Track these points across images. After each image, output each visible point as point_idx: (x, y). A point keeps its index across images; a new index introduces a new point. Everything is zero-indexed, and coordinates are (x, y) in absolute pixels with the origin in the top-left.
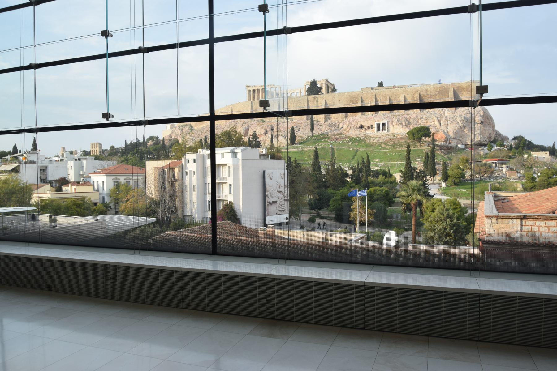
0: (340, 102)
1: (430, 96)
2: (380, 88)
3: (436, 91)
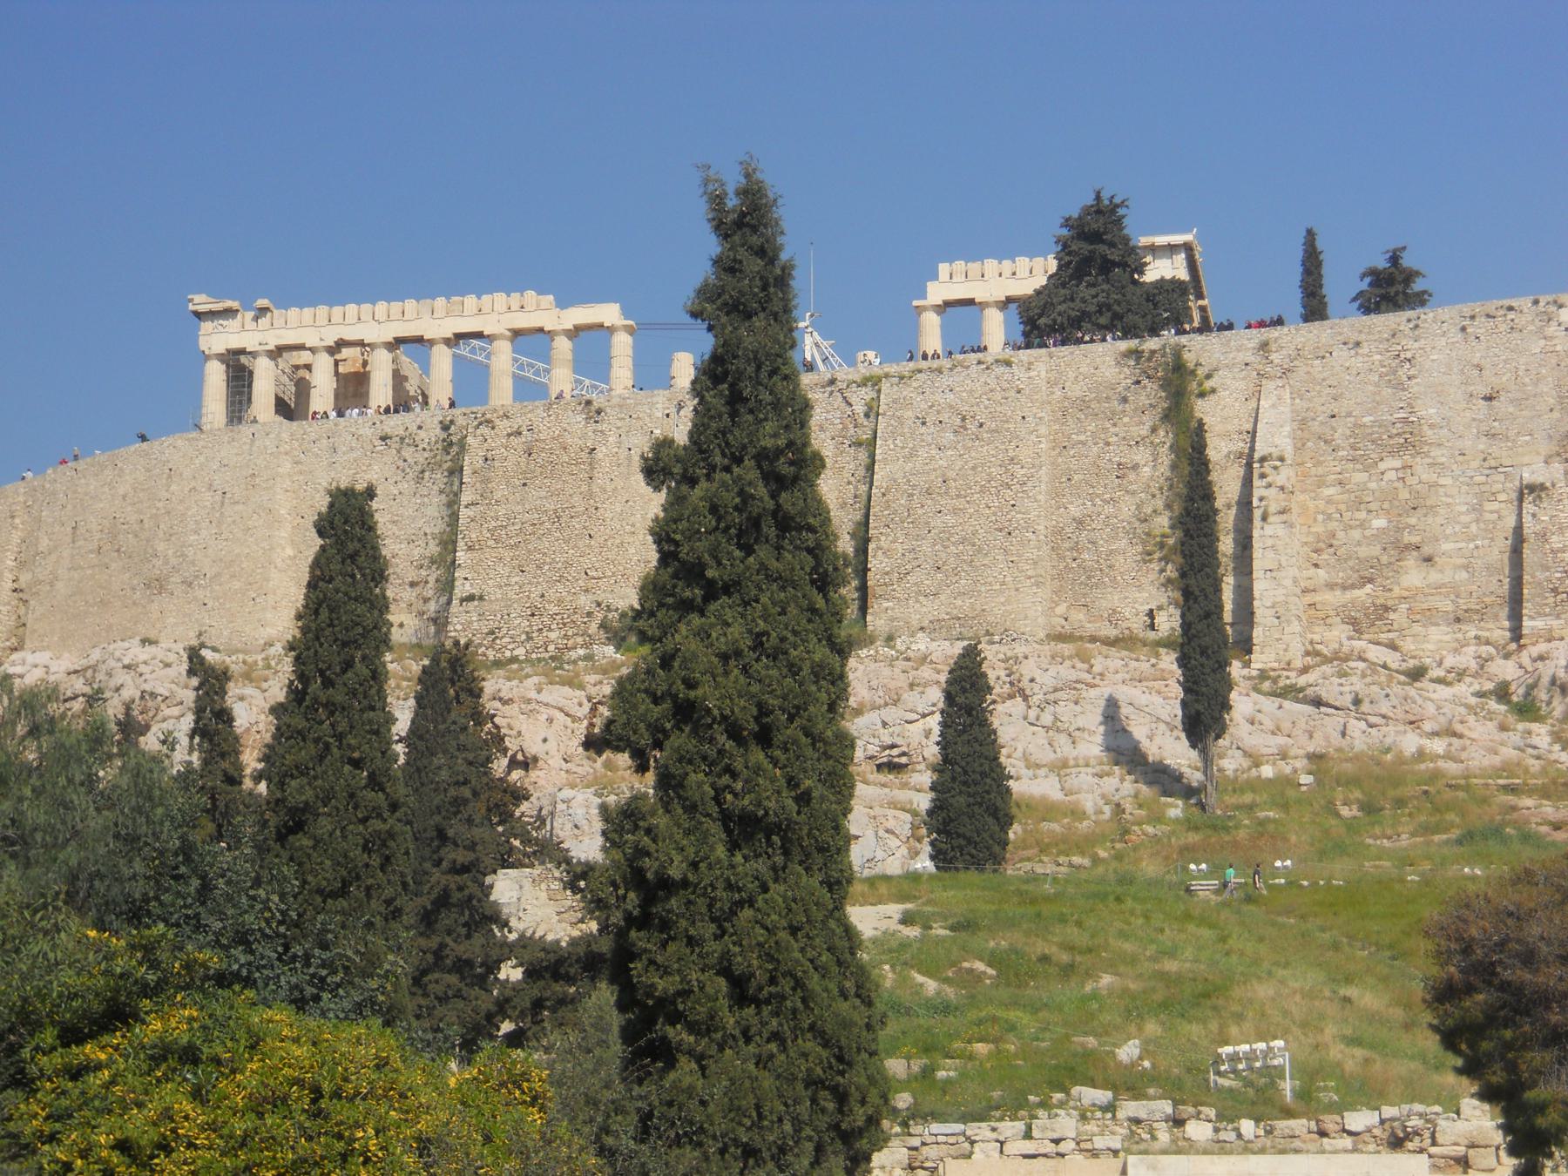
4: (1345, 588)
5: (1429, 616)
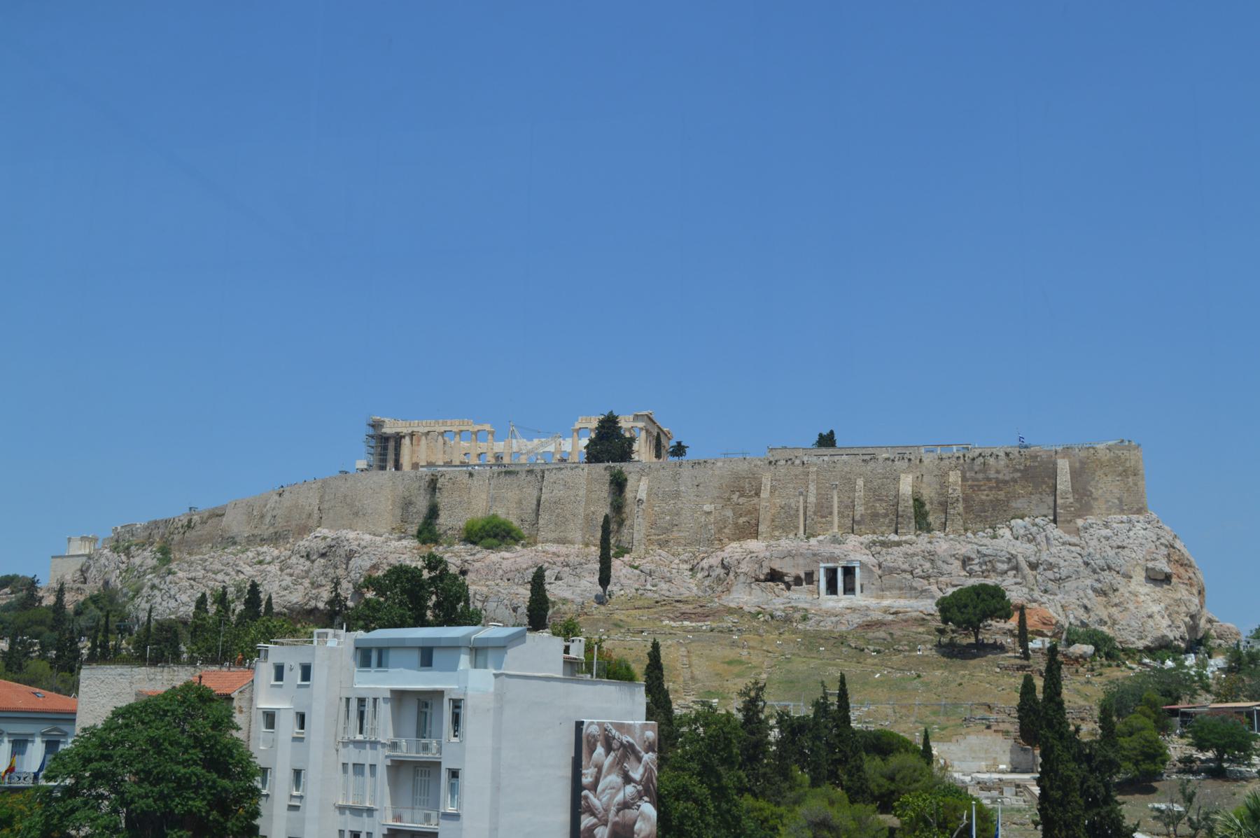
0: (701, 488)
2: (824, 450)
3: (1016, 470)
4: (658, 535)
5: (679, 544)
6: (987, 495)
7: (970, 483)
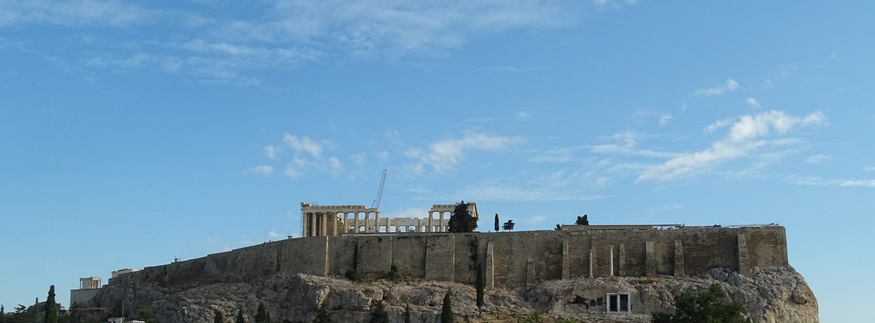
0: (525, 248)
1: (701, 248)
2: (582, 227)
3: (715, 240)
6: (697, 254)
7: (687, 247)
